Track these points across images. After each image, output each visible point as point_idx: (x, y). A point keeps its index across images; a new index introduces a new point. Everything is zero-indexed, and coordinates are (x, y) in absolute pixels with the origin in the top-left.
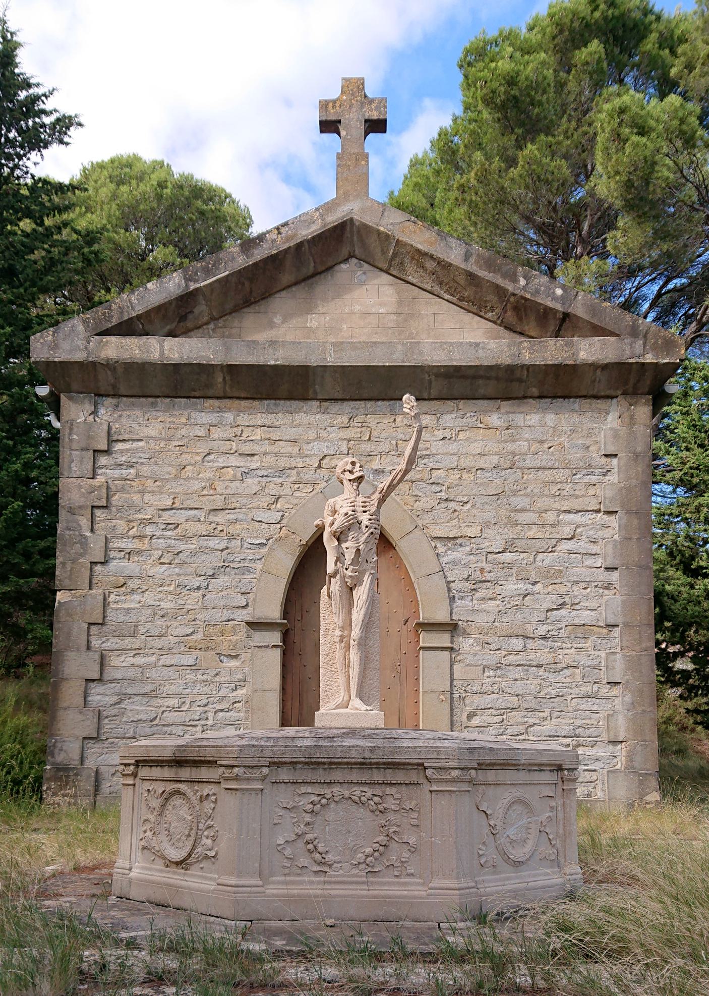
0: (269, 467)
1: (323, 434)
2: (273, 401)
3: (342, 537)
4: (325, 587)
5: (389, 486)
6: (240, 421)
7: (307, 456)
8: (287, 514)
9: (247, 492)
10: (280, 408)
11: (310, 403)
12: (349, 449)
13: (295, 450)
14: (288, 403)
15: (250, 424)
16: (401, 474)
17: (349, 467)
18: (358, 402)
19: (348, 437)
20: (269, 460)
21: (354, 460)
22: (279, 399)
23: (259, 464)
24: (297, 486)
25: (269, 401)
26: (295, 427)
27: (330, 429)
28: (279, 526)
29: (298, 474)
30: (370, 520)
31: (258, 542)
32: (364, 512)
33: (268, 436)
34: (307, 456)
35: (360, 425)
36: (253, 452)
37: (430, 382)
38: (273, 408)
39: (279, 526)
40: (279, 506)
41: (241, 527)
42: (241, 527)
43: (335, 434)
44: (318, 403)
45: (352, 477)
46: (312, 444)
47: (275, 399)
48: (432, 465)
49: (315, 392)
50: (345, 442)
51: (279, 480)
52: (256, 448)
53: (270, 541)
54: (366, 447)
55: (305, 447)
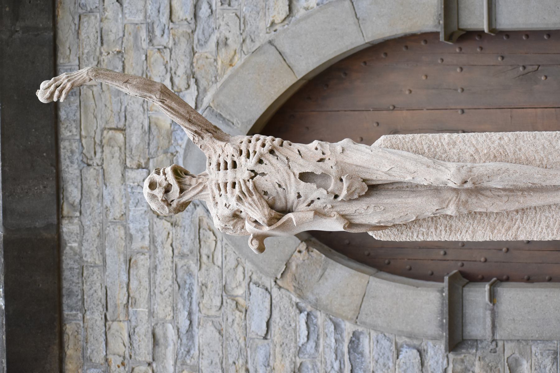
0: (174, 309)
1: (115, 212)
2: (65, 301)
3: (280, 204)
4: (370, 233)
5: (190, 121)
6: (99, 358)
7: (153, 240)
8: (254, 277)
9: (217, 347)
10: (75, 289)
11: (65, 237)
12: (139, 167)
13: (143, 262)
14: (66, 274)
15: (102, 339)
16: (168, 101)
17: (159, 192)
18: (62, 152)
19: (119, 169)
20: (163, 310)
21: (146, 184)
22: (60, 288)
23: (170, 326)
24: (204, 258)
25: (65, 308)
26: (104, 261)
27: (107, 202)
28: (275, 291)
29: (183, 256)
30: (248, 156)
31: (304, 327)
32: (234, 165)
33: (121, 309)
34: (153, 240)
35: (99, 150)
36: (150, 335)
37: (26, 29)
38: (74, 300)
39: (275, 291)
40: (240, 292)
41: (279, 357)
42: (279, 357)
43: (115, 190)
44: (65, 222)
45: (175, 188)
46: (133, 231)
47: (60, 296)
48: (164, 19)
49: (48, 227)
50: (130, 174)
51: (196, 289)
52: (143, 329)
53: (302, 305)
54: (135, 138)
55: (136, 245)
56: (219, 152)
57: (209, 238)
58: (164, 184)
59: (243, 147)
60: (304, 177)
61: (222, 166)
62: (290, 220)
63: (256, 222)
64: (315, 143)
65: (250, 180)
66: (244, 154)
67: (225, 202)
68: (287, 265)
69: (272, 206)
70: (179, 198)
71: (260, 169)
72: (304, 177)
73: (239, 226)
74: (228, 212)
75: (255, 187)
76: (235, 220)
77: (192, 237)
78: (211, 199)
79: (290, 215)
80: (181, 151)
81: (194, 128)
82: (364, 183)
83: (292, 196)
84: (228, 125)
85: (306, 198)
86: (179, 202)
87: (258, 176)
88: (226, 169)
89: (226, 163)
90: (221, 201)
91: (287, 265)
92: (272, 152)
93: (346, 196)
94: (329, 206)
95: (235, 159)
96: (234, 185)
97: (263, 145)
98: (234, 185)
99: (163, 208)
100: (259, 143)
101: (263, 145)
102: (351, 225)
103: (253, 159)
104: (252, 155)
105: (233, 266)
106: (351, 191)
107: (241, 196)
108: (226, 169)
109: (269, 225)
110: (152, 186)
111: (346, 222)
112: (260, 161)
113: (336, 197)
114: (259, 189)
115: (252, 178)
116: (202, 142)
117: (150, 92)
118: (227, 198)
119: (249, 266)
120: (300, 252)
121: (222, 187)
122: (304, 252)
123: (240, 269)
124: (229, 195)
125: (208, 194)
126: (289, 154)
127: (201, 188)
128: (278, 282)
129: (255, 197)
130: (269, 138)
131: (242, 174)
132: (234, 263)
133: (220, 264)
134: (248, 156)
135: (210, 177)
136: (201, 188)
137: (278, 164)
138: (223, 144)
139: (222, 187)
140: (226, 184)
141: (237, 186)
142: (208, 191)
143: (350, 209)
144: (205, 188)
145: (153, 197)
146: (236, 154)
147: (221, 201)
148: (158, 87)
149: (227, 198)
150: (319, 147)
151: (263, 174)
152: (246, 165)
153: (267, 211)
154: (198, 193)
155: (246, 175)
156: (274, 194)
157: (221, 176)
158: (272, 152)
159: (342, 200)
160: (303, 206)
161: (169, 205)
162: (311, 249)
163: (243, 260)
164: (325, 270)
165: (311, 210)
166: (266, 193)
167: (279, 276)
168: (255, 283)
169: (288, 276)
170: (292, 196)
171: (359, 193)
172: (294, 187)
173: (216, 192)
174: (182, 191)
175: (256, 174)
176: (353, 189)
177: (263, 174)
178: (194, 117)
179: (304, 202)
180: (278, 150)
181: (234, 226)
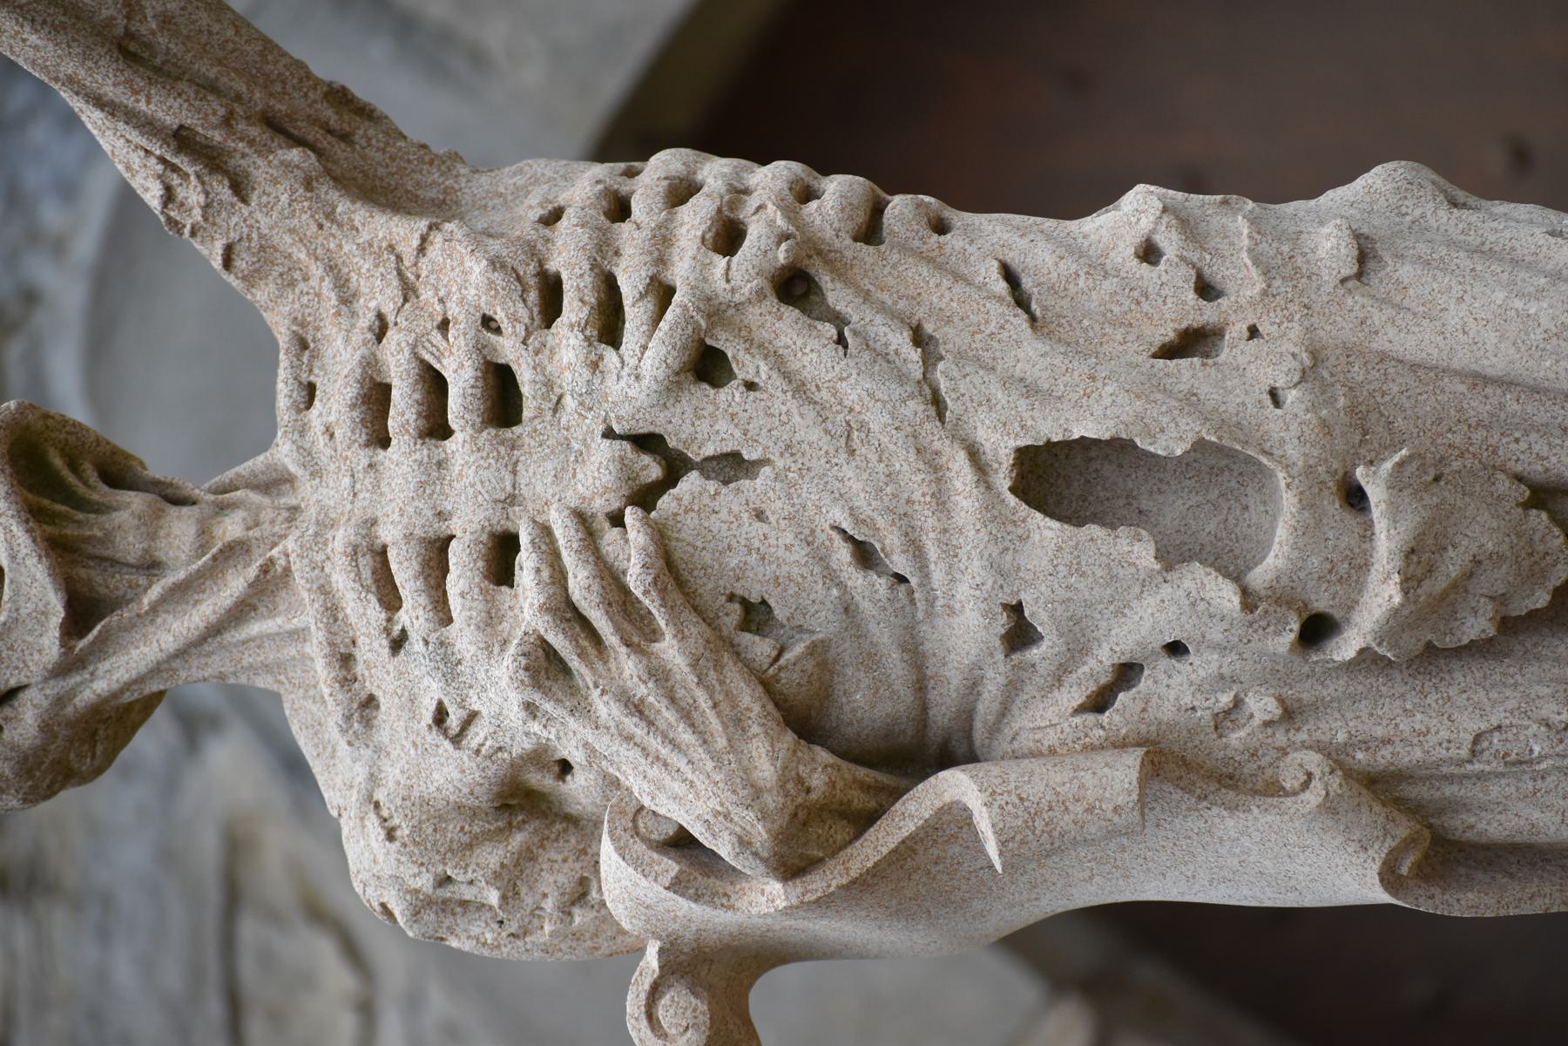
3: (867, 702)
5: (129, 51)
30: (608, 325)
32: (502, 398)
56: (379, 295)
59: (568, 256)
60: (1056, 478)
62: (955, 821)
63: (681, 842)
64: (1140, 208)
65: (631, 516)
66: (574, 309)
67: (432, 691)
69: (804, 720)
71: (705, 422)
72: (1056, 478)
73: (551, 882)
74: (451, 773)
75: (671, 568)
76: (518, 839)
77: (172, 977)
78: (322, 671)
79: (956, 786)
80: (65, 290)
81: (169, 110)
82: (1539, 519)
83: (965, 632)
85: (1077, 650)
86: (60, 701)
87: (690, 483)
88: (436, 428)
89: (434, 384)
90: (406, 686)
92: (794, 286)
93: (1395, 627)
94: (1261, 706)
95: (508, 349)
96: (501, 556)
97: (728, 237)
98: (501, 556)
100: (695, 218)
101: (728, 237)
102: (1442, 851)
103: (649, 352)
104: (635, 314)
106: (1439, 584)
107: (558, 641)
108: (436, 428)
109: (791, 868)
111: (1403, 829)
112: (706, 366)
113: (1316, 630)
114: (706, 587)
115: (645, 497)
116: (236, 221)
118: (448, 663)
124: (463, 637)
125: (298, 635)
126: (938, 297)
127: (235, 584)
129: (670, 650)
130: (769, 180)
131: (567, 471)
134: (608, 325)
135: (311, 495)
136: (235, 584)
137: (854, 387)
138: (404, 231)
140: (436, 553)
141: (527, 561)
143: (1429, 727)
144: (269, 585)
146: (513, 313)
149: (448, 663)
150: (1170, 243)
151: (731, 466)
152: (594, 391)
153: (765, 756)
154: (214, 631)
155: (598, 474)
156: (824, 623)
157: (395, 491)
158: (794, 286)
159: (1366, 657)
160: (1051, 713)
165: (1121, 745)
166: (755, 615)
170: (965, 632)
171: (1501, 600)
172: (977, 563)
173: (364, 614)
174: (84, 612)
175: (676, 467)
176: (1453, 565)
177: (731, 466)
179: (1058, 678)
180: (841, 271)
181: (511, 881)
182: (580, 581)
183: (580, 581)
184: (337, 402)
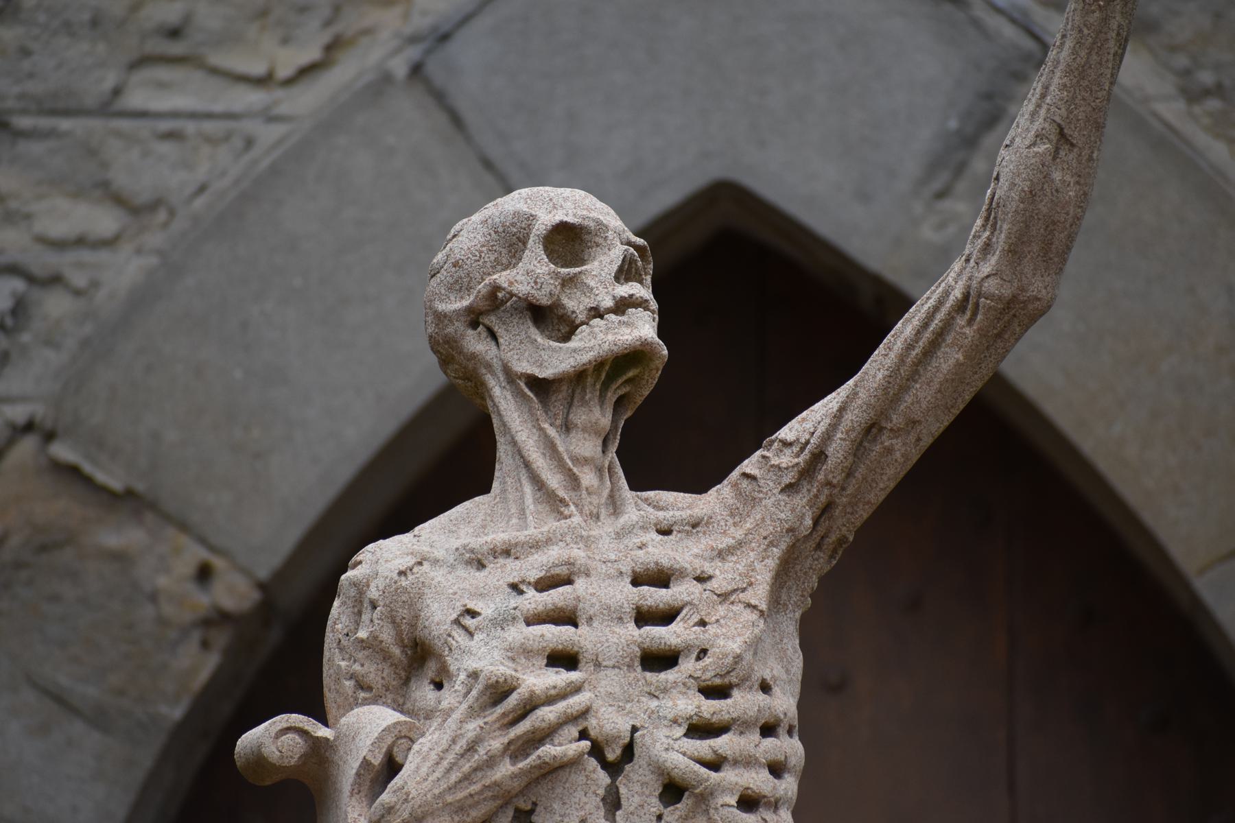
5: (872, 429)
8: (55, 305)
16: (965, 330)
17: (532, 274)
30: (700, 729)
32: (659, 660)
56: (724, 575)
57: (285, 41)
58: (575, 304)
59: (744, 702)
61: (655, 597)
63: (392, 767)
66: (710, 708)
67: (487, 609)
68: (129, 502)
70: (507, 370)
71: (638, 791)
73: (371, 670)
74: (438, 616)
75: (552, 771)
76: (396, 651)
78: (499, 536)
81: (837, 450)
84: (934, 166)
86: (489, 366)
87: (603, 778)
88: (644, 617)
89: (667, 617)
90: (489, 591)
91: (129, 502)
95: (688, 665)
96: (564, 659)
98: (564, 659)
99: (459, 286)
100: (759, 781)
104: (703, 747)
105: (121, 179)
107: (513, 700)
108: (644, 617)
110: (568, 242)
112: (673, 790)
116: (770, 484)
117: (1014, 252)
118: (502, 621)
119: (125, 270)
120: (204, 574)
121: (557, 597)
122: (203, 600)
123: (105, 221)
124: (519, 633)
127: (554, 481)
128: (27, 446)
129: (505, 769)
131: (614, 702)
132: (141, 185)
133: (136, 98)
134: (700, 729)
135: (605, 529)
138: (759, 595)
139: (557, 597)
140: (567, 617)
141: (560, 677)
142: (539, 524)
144: (554, 503)
145: (512, 241)
146: (708, 669)
147: (489, 591)
148: (1037, 286)
149: (502, 621)
151: (613, 802)
154: (527, 465)
155: (612, 722)
161: (474, 318)
162: (221, 638)
163: (155, 239)
164: (99, 719)
167: (62, 451)
168: (20, 308)
169: (60, 507)
173: (533, 566)
174: (541, 387)
175: (614, 769)
177: (613, 802)
178: (889, 451)
182: (548, 714)
183: (548, 714)
184: (660, 552)
